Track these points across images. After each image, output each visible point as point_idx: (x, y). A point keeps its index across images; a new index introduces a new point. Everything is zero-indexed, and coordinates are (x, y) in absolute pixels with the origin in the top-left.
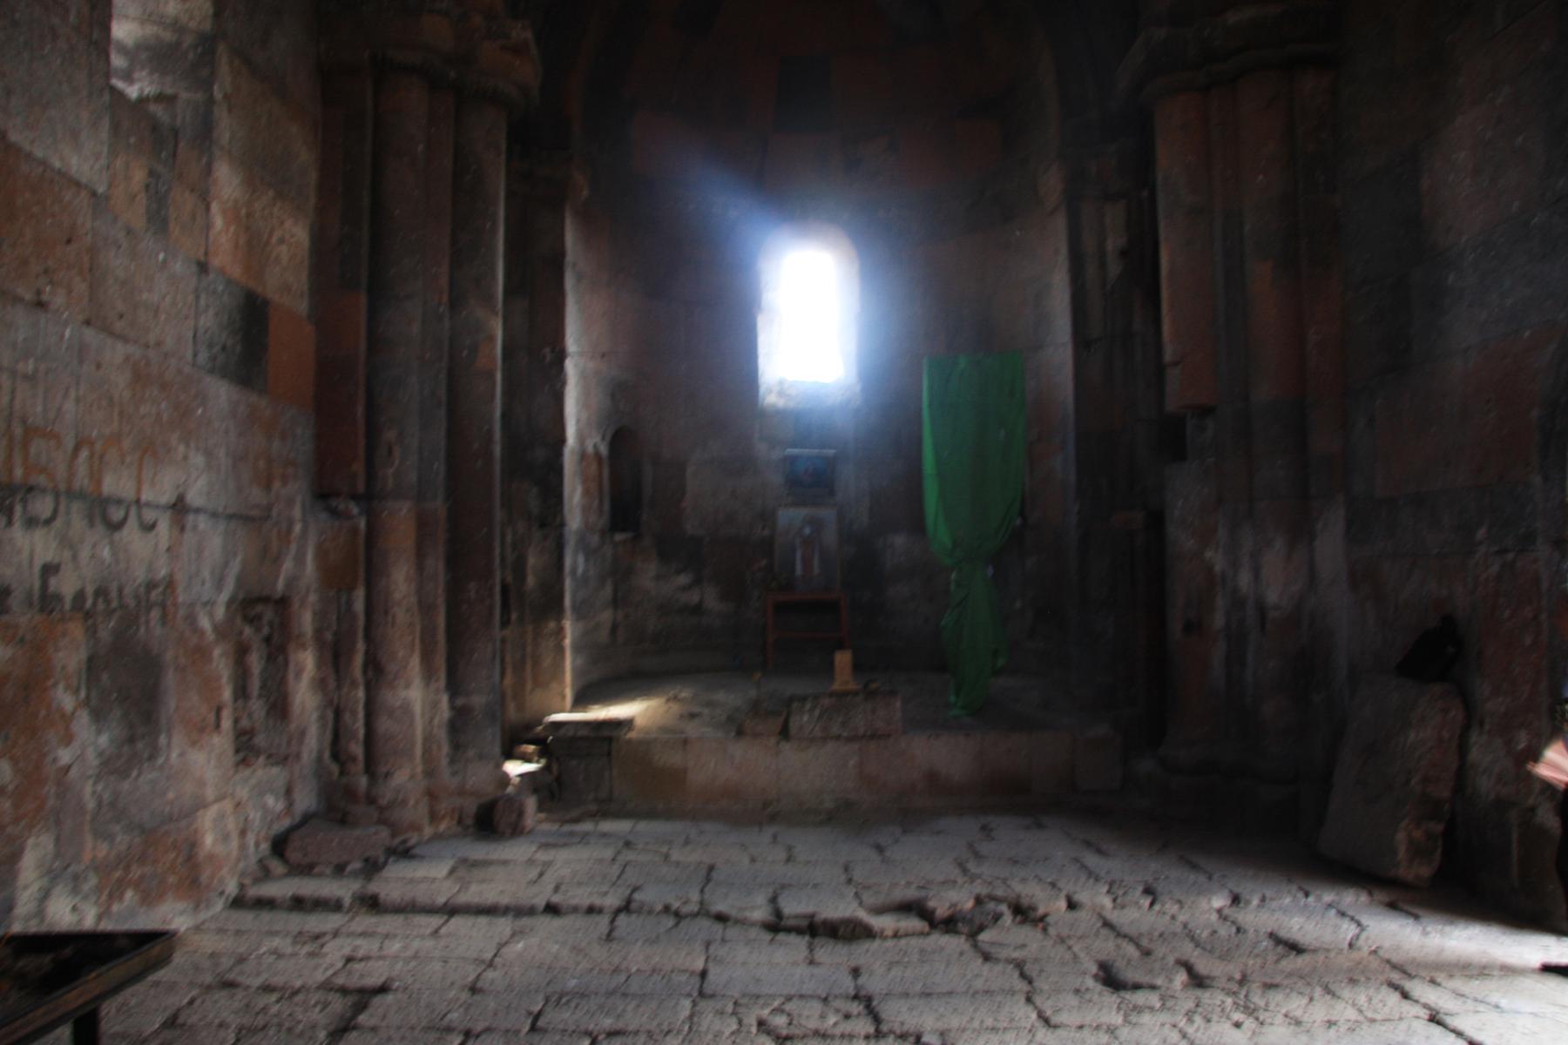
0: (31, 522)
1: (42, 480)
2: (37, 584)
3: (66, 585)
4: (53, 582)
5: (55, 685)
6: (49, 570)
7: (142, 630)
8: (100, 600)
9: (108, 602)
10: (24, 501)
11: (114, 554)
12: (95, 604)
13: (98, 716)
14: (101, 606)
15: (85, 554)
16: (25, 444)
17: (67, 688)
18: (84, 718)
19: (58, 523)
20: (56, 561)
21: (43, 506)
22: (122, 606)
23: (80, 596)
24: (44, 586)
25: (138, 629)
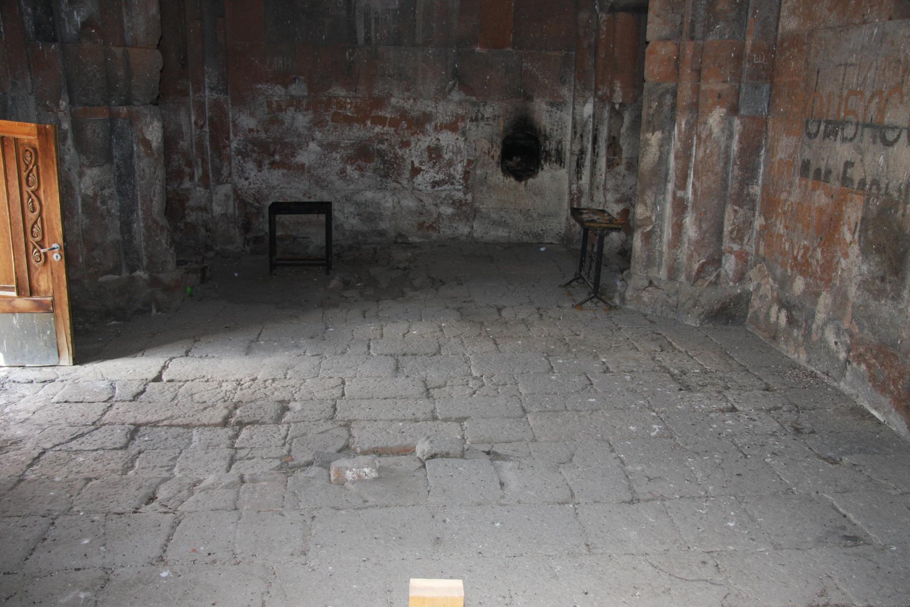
0: (844, 140)
1: (851, 118)
2: (842, 170)
3: (856, 174)
4: (849, 171)
5: (844, 224)
6: (848, 164)
7: (900, 212)
8: (874, 187)
9: (879, 189)
10: (843, 129)
11: (886, 160)
12: (870, 189)
13: (864, 252)
14: (874, 191)
15: (868, 158)
16: (847, 100)
17: (849, 229)
18: (855, 250)
19: (856, 141)
20: (853, 161)
21: (849, 131)
22: (887, 194)
23: (862, 183)
24: (845, 172)
25: (896, 212)
